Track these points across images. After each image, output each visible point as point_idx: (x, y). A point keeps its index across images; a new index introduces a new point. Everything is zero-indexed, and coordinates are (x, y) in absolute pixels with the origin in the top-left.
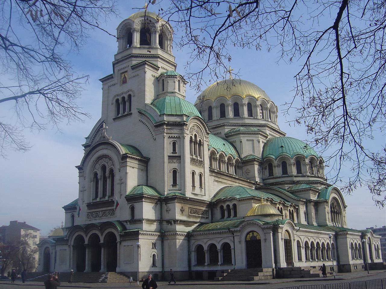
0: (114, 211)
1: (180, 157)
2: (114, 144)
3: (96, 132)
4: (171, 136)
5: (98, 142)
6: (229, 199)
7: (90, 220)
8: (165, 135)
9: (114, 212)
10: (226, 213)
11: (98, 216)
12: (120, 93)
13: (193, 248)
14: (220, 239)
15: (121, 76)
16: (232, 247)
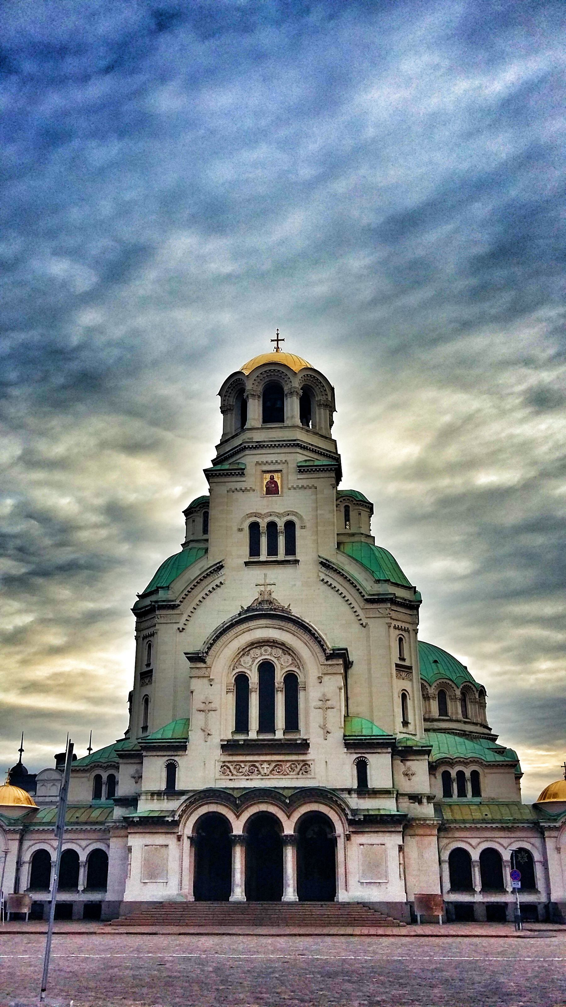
0: (307, 764)
1: (410, 668)
2: (308, 624)
3: (198, 580)
4: (397, 626)
5: (249, 609)
6: (466, 761)
7: (230, 780)
8: (389, 620)
9: (307, 766)
10: (455, 786)
11: (256, 772)
12: (263, 513)
13: (446, 856)
14: (508, 841)
15: (262, 479)
16: (537, 856)
